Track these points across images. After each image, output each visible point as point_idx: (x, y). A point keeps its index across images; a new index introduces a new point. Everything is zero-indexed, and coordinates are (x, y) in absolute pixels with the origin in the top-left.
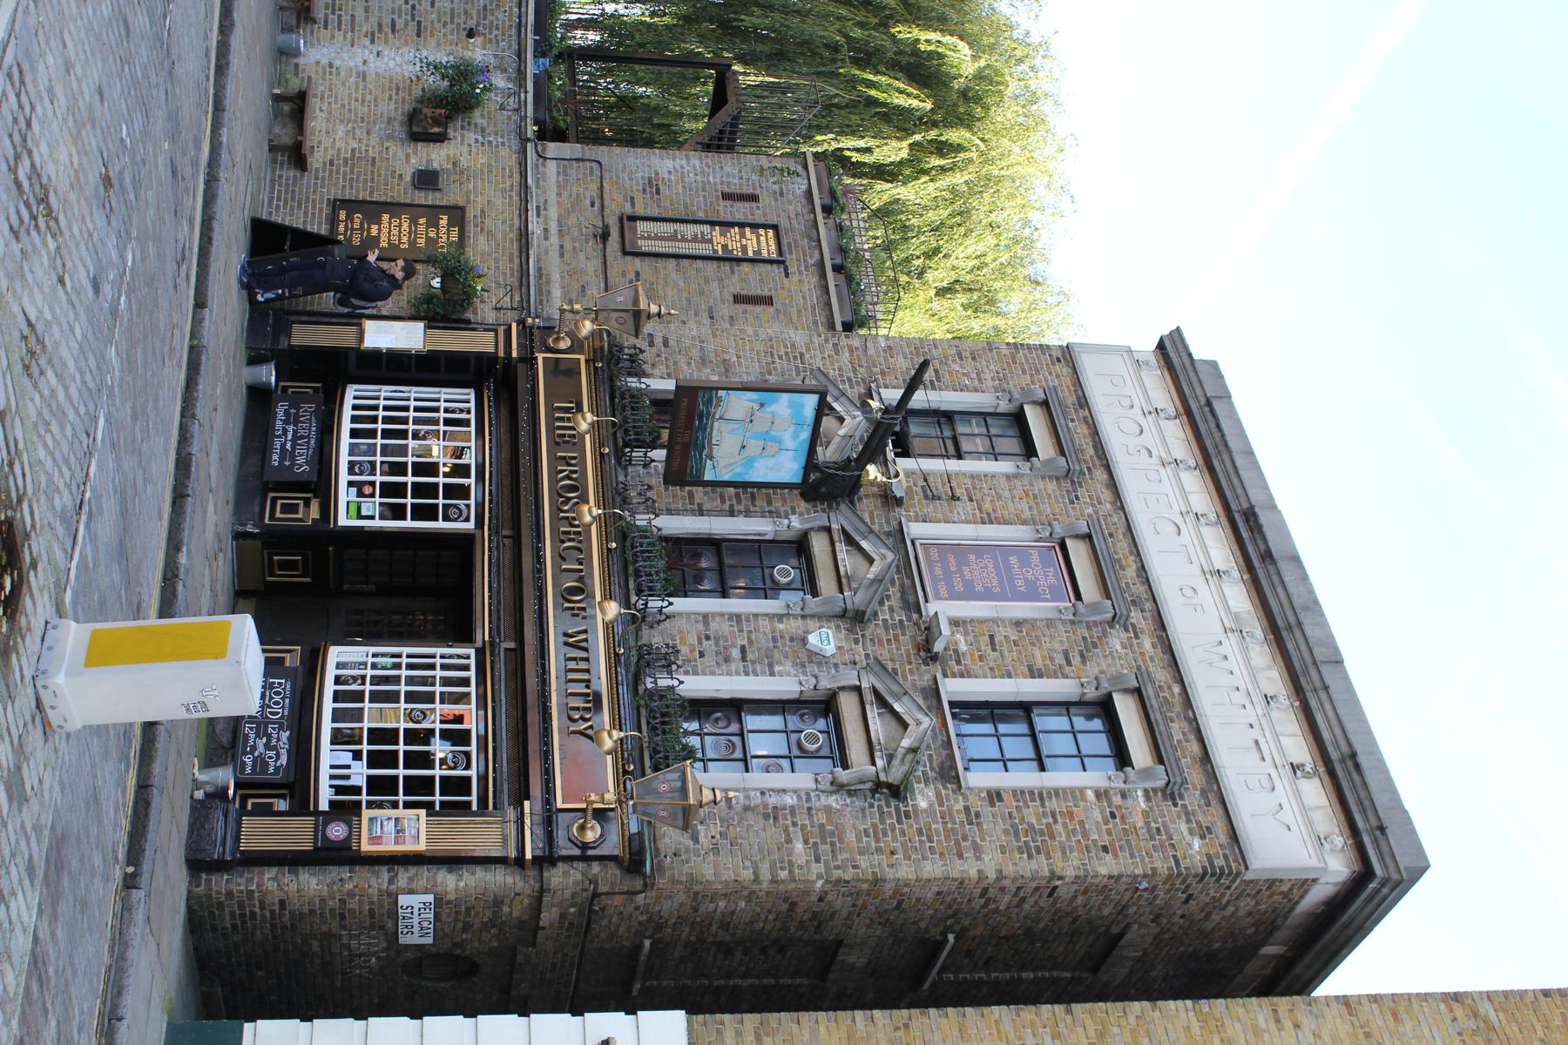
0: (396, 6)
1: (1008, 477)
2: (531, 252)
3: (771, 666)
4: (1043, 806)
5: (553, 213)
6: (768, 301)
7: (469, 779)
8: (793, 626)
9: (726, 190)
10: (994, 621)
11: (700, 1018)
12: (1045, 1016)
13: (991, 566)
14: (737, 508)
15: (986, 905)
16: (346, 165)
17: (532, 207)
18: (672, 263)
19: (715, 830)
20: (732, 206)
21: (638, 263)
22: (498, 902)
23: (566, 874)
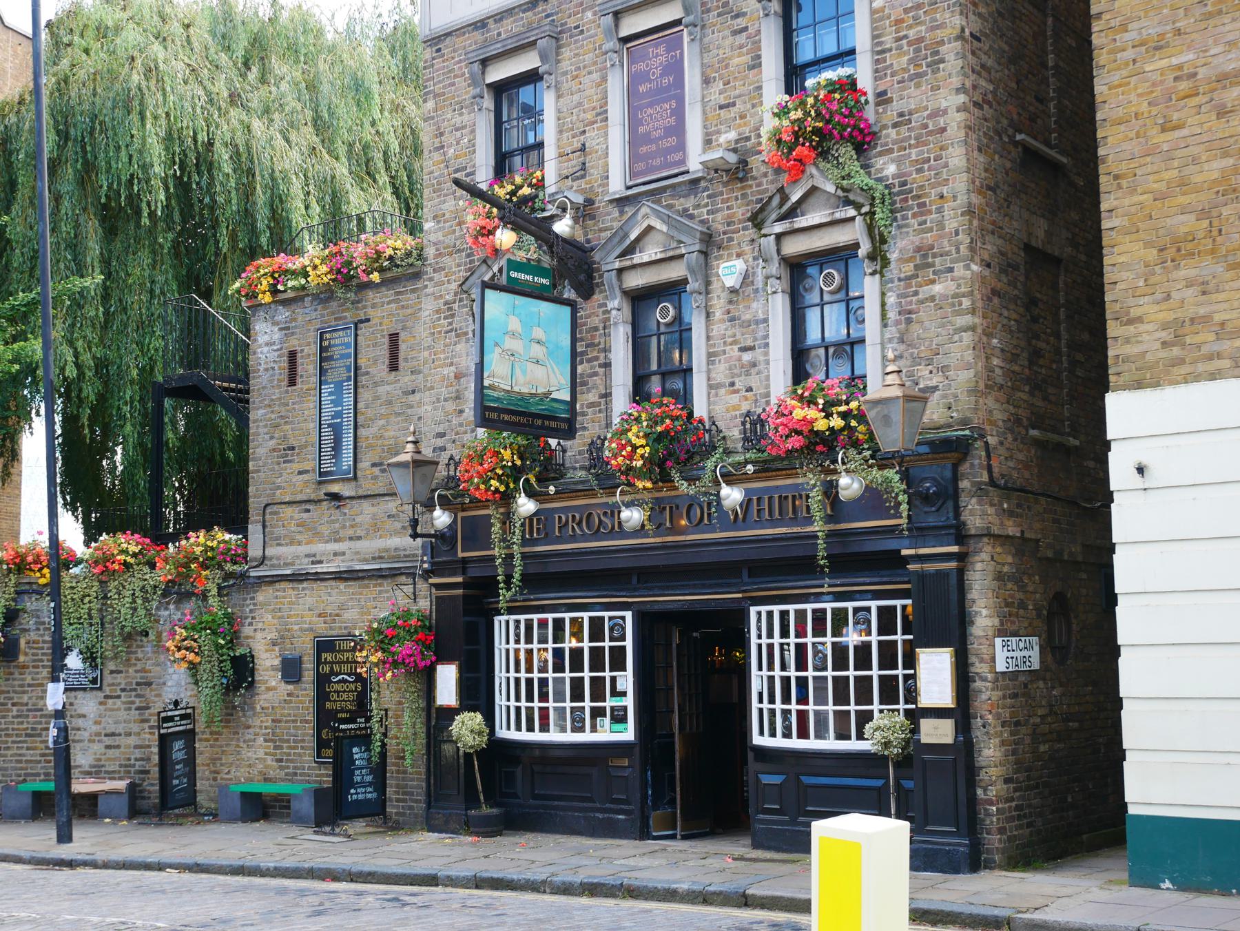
0: (123, 707)
1: (559, 97)
2: (358, 568)
3: (757, 322)
4: (890, 50)
5: (319, 548)
6: (394, 338)
7: (880, 609)
8: (719, 304)
9: (286, 383)
10: (704, 104)
11: (1112, 378)
12: (1104, 41)
13: (650, 111)
14: (602, 361)
15: (989, 103)
16: (281, 747)
17: (314, 569)
19: (923, 371)
20: (302, 376)
21: (364, 465)
22: (999, 577)
23: (972, 513)
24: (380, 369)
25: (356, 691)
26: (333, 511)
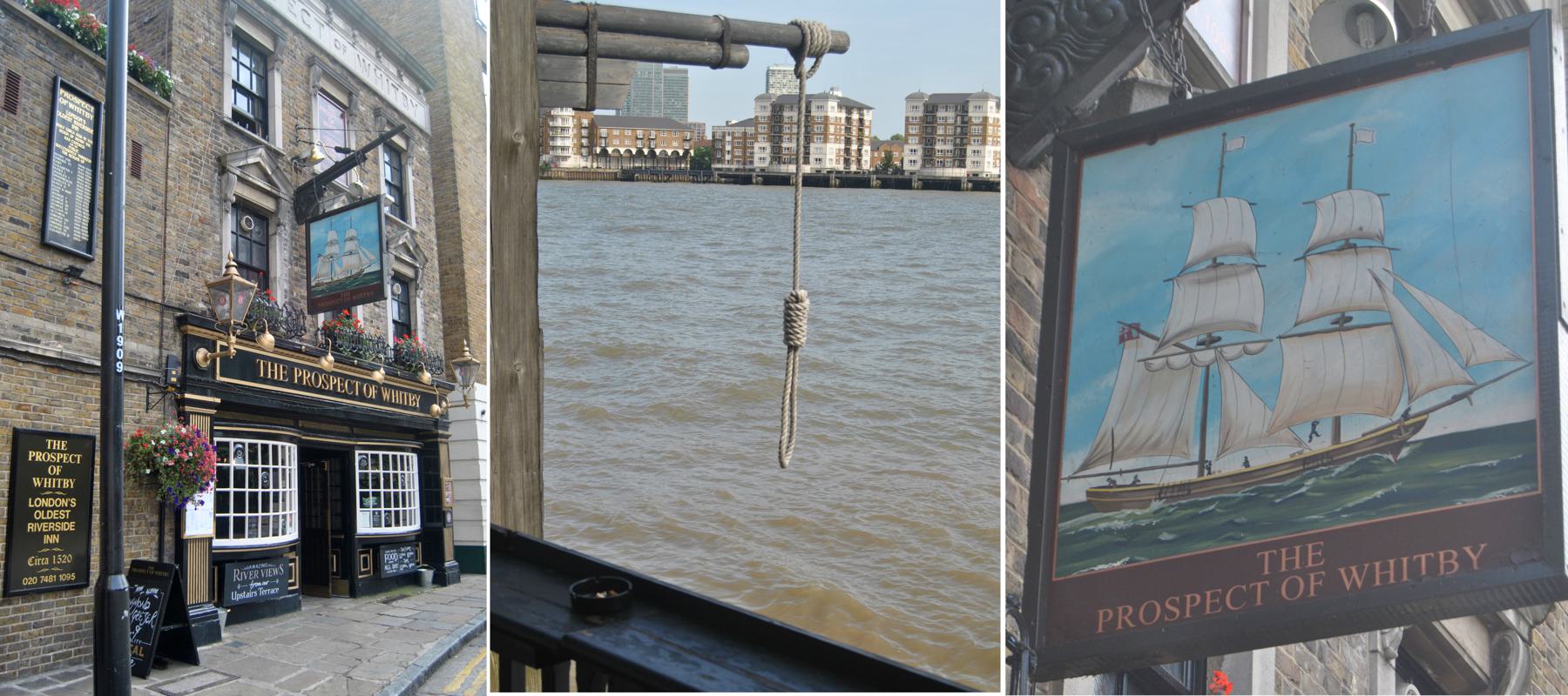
5: (33, 323)
25: (69, 508)
26: (58, 286)
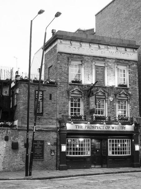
1: (84, 69)
18: (44, 108)
24: (48, 99)
